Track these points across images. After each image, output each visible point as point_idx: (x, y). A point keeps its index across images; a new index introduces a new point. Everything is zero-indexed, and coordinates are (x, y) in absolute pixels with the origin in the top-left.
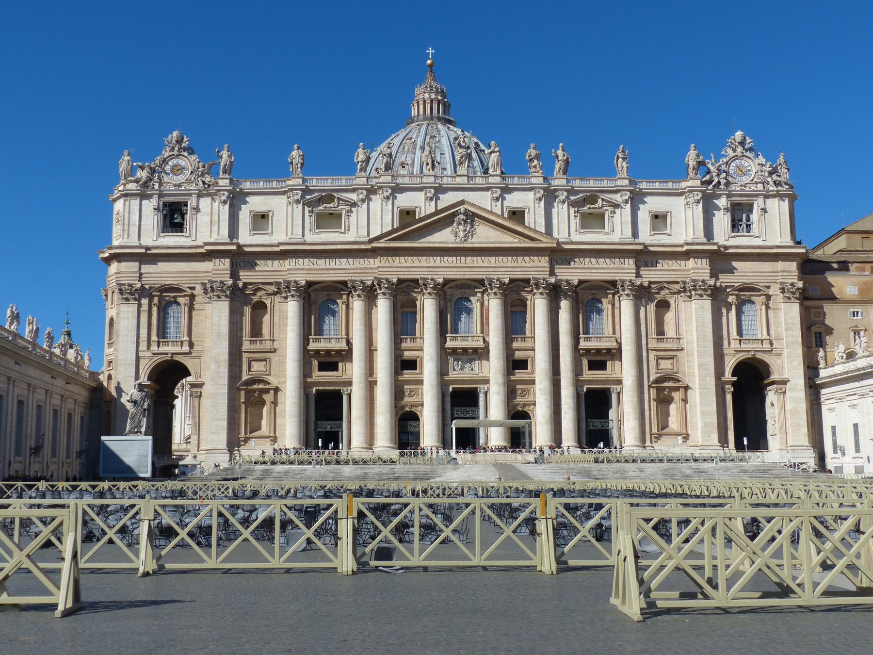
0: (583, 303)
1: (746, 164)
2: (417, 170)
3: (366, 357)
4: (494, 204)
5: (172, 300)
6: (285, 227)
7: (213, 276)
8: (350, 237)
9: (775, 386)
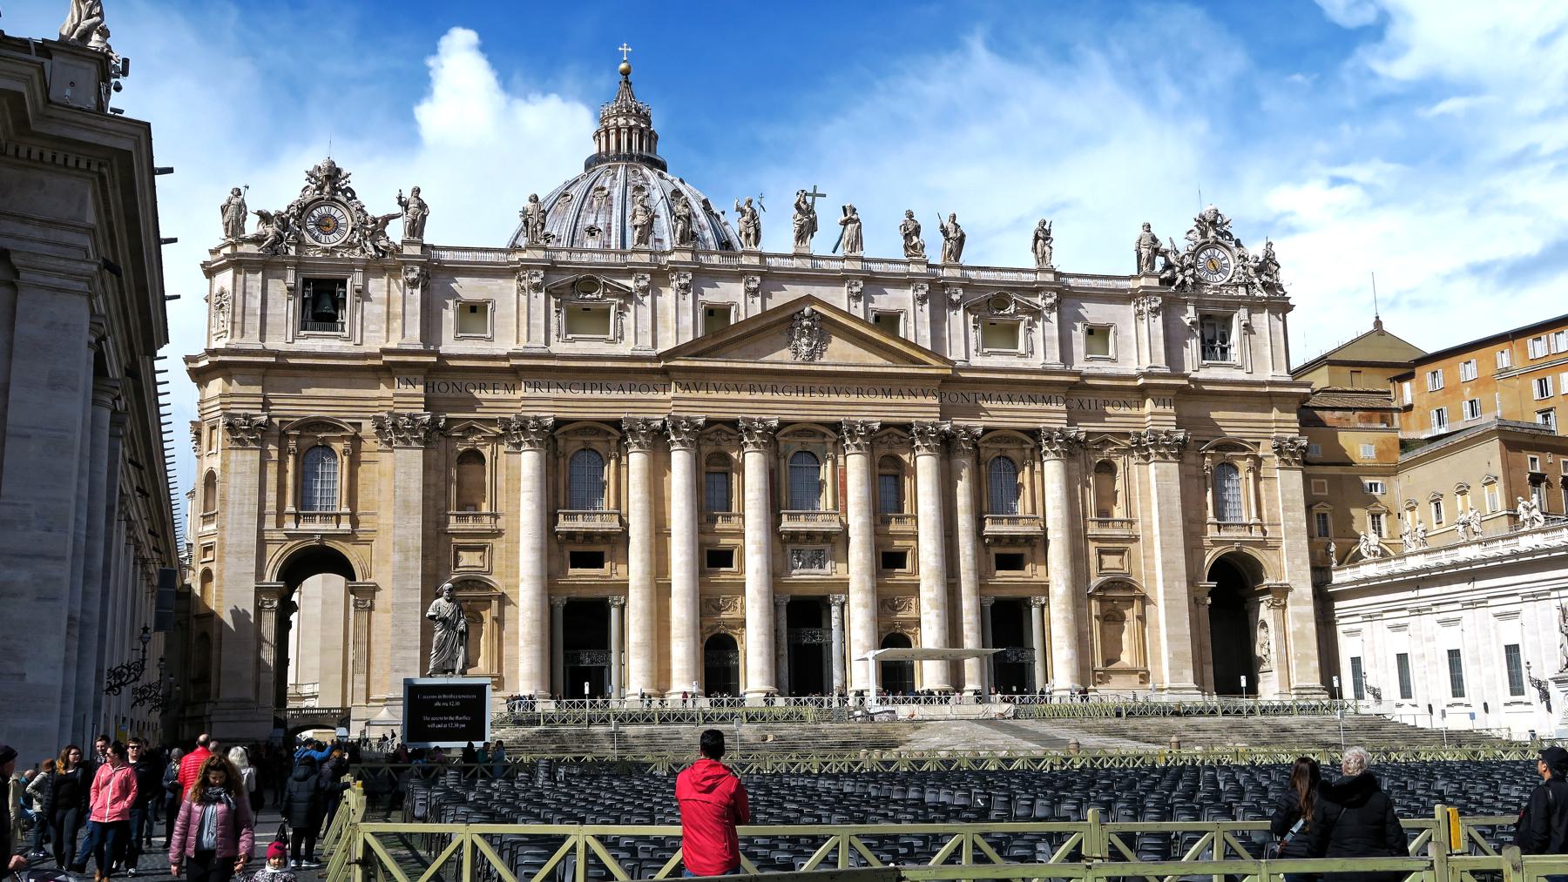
1: (1221, 256)
2: (616, 241)
3: (651, 546)
4: (853, 304)
5: (319, 444)
6: (515, 328)
7: (396, 405)
8: (624, 349)
9: (1269, 597)
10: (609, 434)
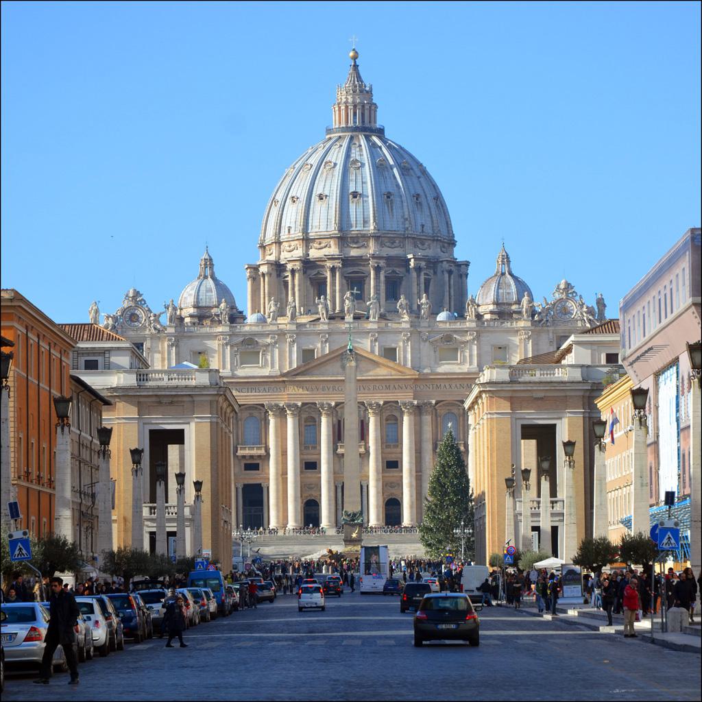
0: (440, 417)
8: (266, 372)
10: (260, 410)
